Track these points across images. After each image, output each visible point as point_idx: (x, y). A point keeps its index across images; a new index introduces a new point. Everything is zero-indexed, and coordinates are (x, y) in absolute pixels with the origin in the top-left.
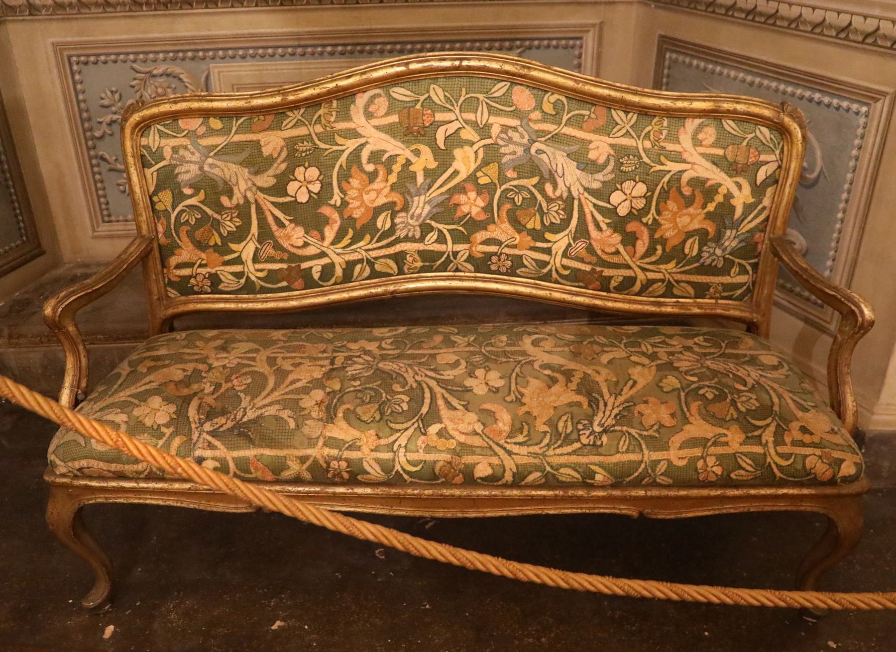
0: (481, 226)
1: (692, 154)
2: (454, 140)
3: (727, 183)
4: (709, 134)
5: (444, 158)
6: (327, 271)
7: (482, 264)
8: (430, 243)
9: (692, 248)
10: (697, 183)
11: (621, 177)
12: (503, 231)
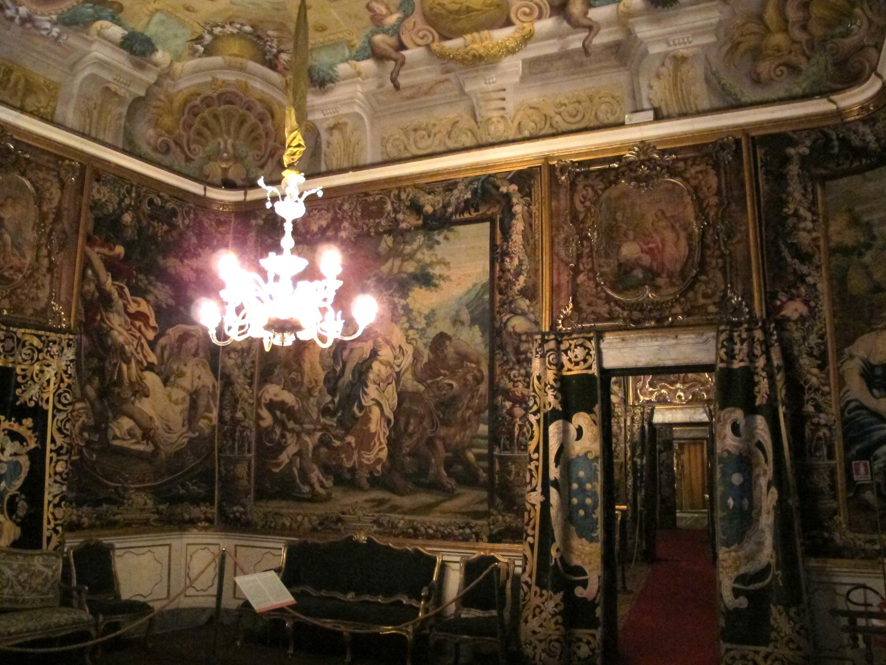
1: (38, 565)
3: (46, 570)
4: (41, 559)
9: (39, 588)
10: (39, 571)
11: (21, 572)
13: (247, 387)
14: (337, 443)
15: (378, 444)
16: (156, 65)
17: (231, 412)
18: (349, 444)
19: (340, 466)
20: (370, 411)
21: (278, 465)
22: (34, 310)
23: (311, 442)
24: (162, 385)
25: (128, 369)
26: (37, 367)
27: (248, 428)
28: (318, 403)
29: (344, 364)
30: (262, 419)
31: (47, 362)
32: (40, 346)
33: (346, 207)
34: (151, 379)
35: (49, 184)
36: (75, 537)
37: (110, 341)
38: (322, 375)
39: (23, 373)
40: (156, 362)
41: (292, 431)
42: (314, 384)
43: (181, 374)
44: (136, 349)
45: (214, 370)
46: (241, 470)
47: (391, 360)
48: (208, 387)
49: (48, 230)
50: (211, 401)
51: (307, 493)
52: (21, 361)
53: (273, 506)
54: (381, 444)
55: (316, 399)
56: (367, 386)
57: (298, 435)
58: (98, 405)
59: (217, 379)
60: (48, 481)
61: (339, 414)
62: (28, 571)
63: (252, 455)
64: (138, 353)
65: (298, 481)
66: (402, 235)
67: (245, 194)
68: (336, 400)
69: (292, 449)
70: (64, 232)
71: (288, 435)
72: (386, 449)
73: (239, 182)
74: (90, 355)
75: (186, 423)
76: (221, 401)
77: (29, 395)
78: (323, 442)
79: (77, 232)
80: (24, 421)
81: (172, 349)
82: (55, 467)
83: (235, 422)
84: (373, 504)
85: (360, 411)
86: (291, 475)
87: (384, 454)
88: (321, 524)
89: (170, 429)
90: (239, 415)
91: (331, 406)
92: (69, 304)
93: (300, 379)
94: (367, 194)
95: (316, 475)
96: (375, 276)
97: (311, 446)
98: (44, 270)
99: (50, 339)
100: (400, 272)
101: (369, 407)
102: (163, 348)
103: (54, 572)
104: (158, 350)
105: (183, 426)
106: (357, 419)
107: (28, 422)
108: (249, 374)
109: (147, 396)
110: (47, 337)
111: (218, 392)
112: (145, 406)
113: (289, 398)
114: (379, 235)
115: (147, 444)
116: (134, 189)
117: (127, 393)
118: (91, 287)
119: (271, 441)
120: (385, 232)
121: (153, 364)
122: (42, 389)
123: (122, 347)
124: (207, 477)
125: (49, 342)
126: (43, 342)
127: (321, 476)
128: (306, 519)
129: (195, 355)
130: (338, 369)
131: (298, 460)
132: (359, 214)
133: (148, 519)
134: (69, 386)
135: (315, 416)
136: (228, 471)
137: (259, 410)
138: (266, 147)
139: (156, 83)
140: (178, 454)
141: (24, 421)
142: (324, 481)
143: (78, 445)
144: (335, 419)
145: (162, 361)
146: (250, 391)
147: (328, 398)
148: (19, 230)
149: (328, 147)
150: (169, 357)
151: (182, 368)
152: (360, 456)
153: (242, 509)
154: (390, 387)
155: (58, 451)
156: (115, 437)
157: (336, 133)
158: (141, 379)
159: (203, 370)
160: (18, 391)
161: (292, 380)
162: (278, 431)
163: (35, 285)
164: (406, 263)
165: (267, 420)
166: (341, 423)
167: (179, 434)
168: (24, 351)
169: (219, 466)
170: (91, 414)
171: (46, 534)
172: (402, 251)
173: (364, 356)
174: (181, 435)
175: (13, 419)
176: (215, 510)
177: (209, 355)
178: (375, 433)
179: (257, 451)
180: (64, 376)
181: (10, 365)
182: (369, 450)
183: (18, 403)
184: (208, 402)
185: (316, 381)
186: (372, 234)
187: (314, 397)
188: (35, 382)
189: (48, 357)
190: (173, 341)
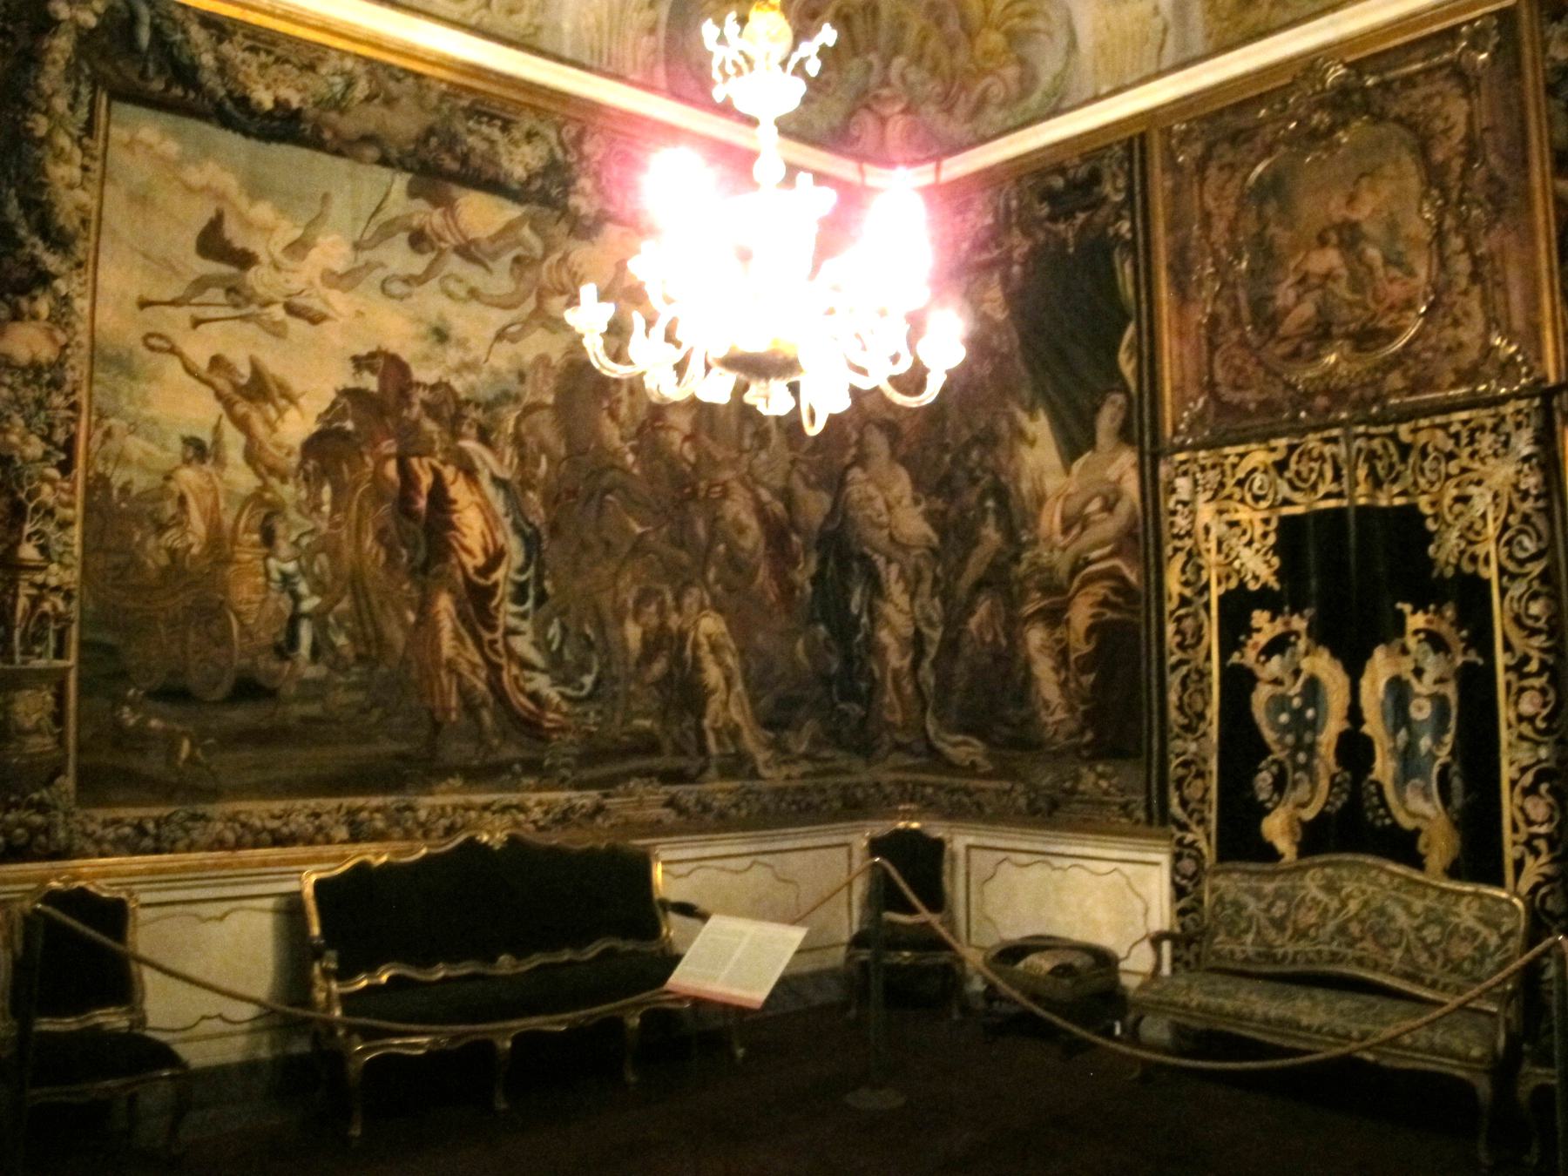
0: (1362, 939)
2: (1349, 896)
3: (1484, 931)
5: (1344, 904)
7: (1360, 962)
8: (1334, 946)
9: (1467, 966)
10: (1468, 929)
11: (1428, 922)
12: (1368, 944)
22: (1456, 371)
31: (1474, 476)
35: (1437, 101)
60: (1505, 735)
62: (1440, 921)
70: (1491, 179)
82: (1516, 703)
92: (1535, 330)
98: (1463, 282)
103: (1505, 938)
148: (1393, 227)
163: (1448, 320)
171: (1510, 853)
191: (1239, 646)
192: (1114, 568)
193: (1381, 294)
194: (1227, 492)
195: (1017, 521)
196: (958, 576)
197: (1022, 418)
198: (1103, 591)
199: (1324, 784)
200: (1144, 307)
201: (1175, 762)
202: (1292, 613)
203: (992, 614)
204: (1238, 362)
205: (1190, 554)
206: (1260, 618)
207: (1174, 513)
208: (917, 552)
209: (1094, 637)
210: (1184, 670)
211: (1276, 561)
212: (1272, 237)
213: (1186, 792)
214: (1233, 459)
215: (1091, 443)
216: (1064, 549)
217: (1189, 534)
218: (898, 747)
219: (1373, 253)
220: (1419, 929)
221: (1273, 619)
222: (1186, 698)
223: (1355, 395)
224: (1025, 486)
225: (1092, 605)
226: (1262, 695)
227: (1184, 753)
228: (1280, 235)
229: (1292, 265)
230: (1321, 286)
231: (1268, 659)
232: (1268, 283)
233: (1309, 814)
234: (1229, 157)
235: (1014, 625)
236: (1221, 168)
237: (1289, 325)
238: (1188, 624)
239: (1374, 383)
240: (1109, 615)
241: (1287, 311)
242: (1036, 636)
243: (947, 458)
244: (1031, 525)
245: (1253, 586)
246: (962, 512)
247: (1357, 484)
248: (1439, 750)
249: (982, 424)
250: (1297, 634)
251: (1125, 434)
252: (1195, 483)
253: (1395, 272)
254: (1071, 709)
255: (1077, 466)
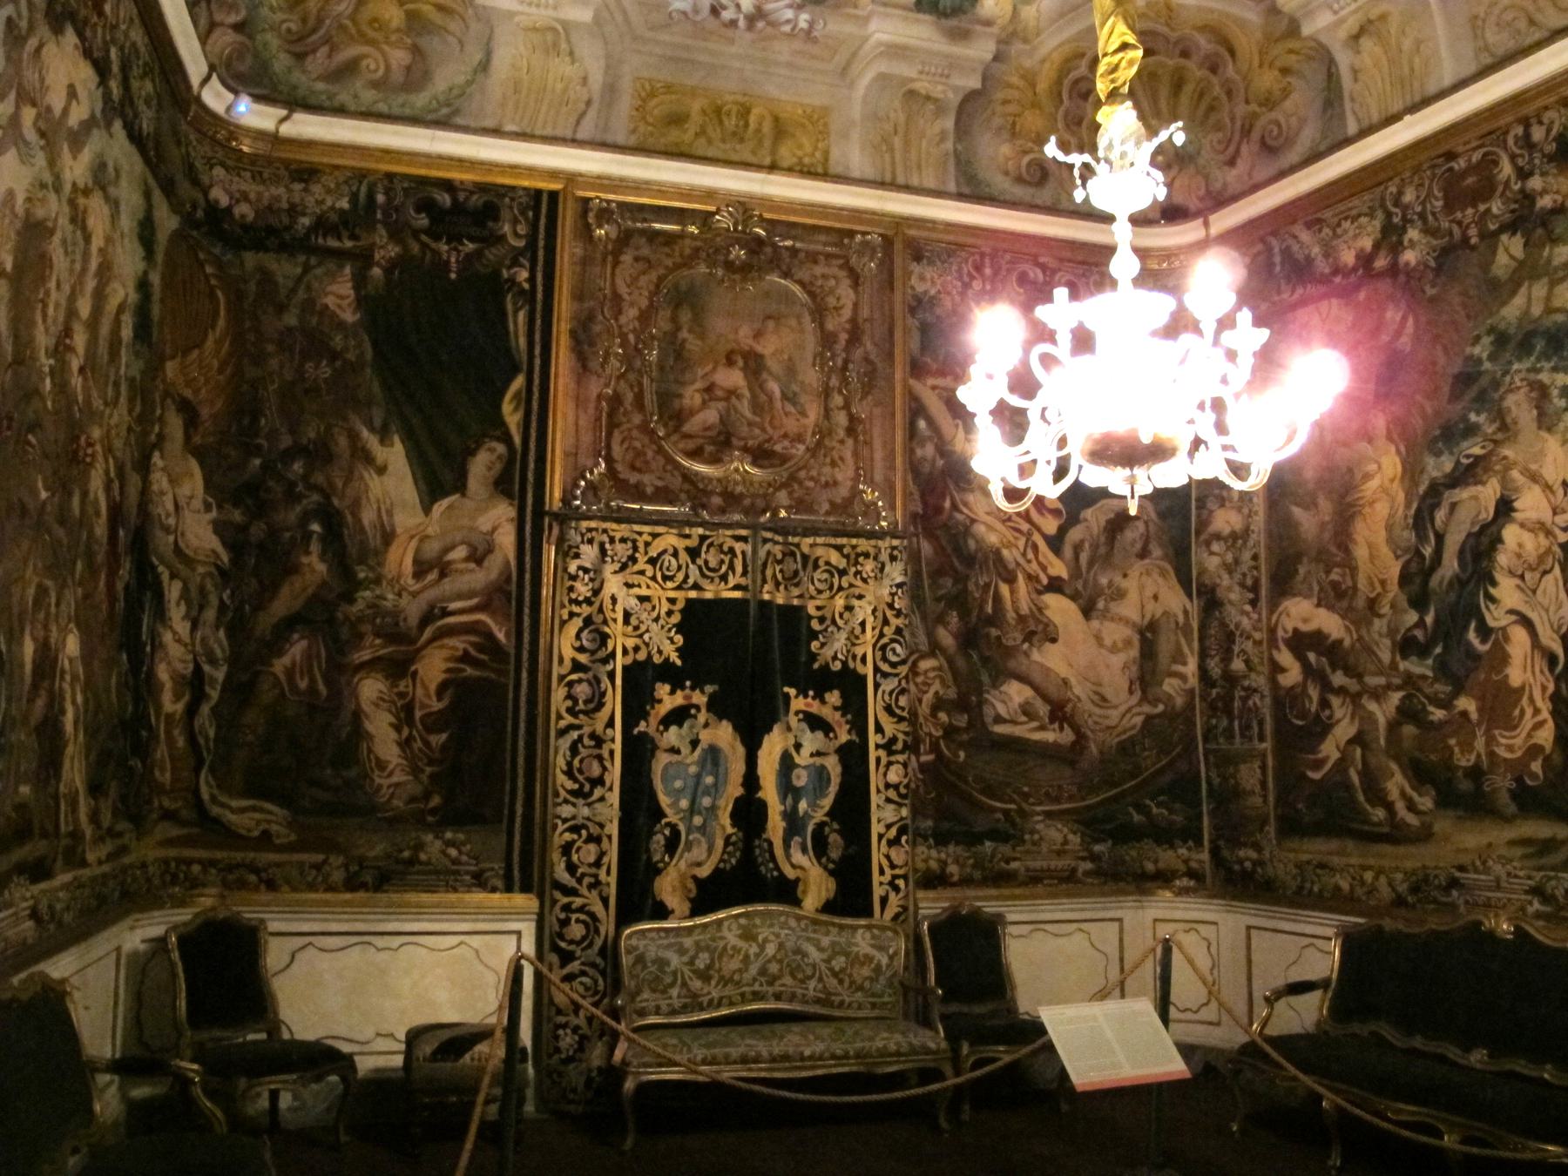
1: (862, 944)
2: (766, 941)
4: (868, 935)
5: (762, 947)
6: (711, 1002)
7: (778, 997)
8: (757, 987)
12: (788, 980)
13: (1248, 608)
14: (1438, 714)
15: (1529, 712)
16: (988, 23)
17: (1223, 660)
18: (1464, 714)
19: (1449, 766)
20: (1507, 639)
21: (1318, 764)
22: (832, 503)
23: (1382, 712)
24: (1080, 616)
25: (1012, 592)
26: (840, 602)
27: (1255, 691)
28: (1391, 632)
29: (1440, 538)
30: (1283, 670)
31: (857, 591)
32: (842, 564)
33: (1409, 196)
34: (1059, 608)
35: (832, 282)
36: (935, 900)
37: (972, 544)
38: (1394, 570)
39: (819, 613)
40: (1065, 575)
41: (1341, 691)
42: (1379, 589)
43: (1120, 595)
44: (1024, 554)
45: (1185, 581)
46: (1248, 776)
47: (1547, 516)
48: (1175, 616)
49: (840, 362)
50: (1183, 641)
51: (1379, 824)
52: (814, 593)
53: (1314, 849)
54: (1537, 711)
55: (1385, 621)
56: (1494, 583)
57: (1355, 698)
58: (961, 663)
59: (1190, 596)
60: (875, 799)
61: (1438, 650)
63: (1267, 745)
64: (1029, 561)
65: (1361, 798)
66: (1544, 224)
67: (1206, 224)
68: (1429, 619)
69: (1344, 730)
70: (867, 360)
71: (1335, 701)
72: (1550, 724)
73: (1193, 204)
74: (937, 574)
75: (1137, 686)
76: (1201, 639)
77: (831, 649)
78: (1409, 713)
79: (890, 355)
80: (827, 696)
81: (1095, 547)
82: (885, 774)
83: (1231, 679)
84: (1530, 850)
85: (1484, 641)
86: (1348, 786)
87: (1546, 736)
88: (1415, 889)
89: (1104, 699)
90: (1238, 665)
91: (1419, 634)
92: (892, 487)
93: (1350, 583)
94: (1451, 156)
95: (1396, 783)
96: (1492, 330)
97: (1382, 721)
98: (841, 433)
99: (859, 550)
100: (1549, 310)
101: (1504, 629)
102: (1077, 548)
104: (1068, 551)
105: (1131, 692)
106: (1475, 657)
107: (834, 697)
108: (1249, 582)
109: (1054, 640)
110: (854, 547)
111: (1195, 625)
112: (1051, 659)
113: (1331, 624)
114: (1490, 238)
115: (1062, 729)
116: (987, 260)
117: (1014, 637)
118: (929, 451)
119: (1303, 714)
120: (1503, 229)
121: (1059, 578)
122: (853, 639)
123: (998, 553)
124: (1183, 789)
125: (858, 555)
126: (847, 557)
127: (1408, 790)
128: (1383, 880)
129: (1143, 554)
130: (1428, 551)
131: (1358, 752)
132: (1439, 204)
133: (1074, 870)
134: (898, 631)
135: (1385, 656)
136: (1225, 779)
137: (1275, 653)
138: (1233, 119)
139: (997, 58)
140: (1126, 748)
141: (827, 696)
142: (1415, 795)
143: (930, 735)
144: (1430, 662)
145: (1076, 572)
146: (1255, 616)
147: (1412, 617)
148: (791, 370)
149: (1356, 80)
150: (1091, 563)
151: (1118, 579)
152: (1491, 740)
153: (1253, 855)
154: (1549, 577)
155: (888, 747)
156: (999, 720)
157: (1367, 43)
158: (1040, 610)
159: (1160, 580)
160: (814, 645)
161: (1335, 585)
162: (1314, 693)
163: (828, 460)
164: (1559, 289)
165: (1293, 674)
166: (1443, 669)
167: (1123, 708)
168: (817, 575)
169: (1208, 770)
170: (949, 677)
171: (878, 892)
172: (1549, 261)
173: (1483, 516)
174: (1129, 710)
175: (811, 693)
176: (1205, 856)
177: (1171, 551)
178: (1522, 688)
179: (1278, 732)
180: (889, 613)
181: (796, 602)
182: (1511, 725)
183: (816, 666)
184: (1178, 643)
185: (1383, 583)
186: (1474, 241)
187: (1380, 616)
188: (839, 628)
189: (859, 583)
190: (1095, 531)
191: (645, 716)
192: (477, 622)
193: (776, 423)
194: (636, 568)
195: (353, 550)
196: (259, 607)
197: (371, 440)
198: (461, 646)
199: (720, 843)
200: (537, 362)
201: (561, 828)
202: (693, 688)
203: (309, 656)
204: (638, 444)
205: (588, 621)
206: (663, 690)
207: (574, 578)
208: (201, 570)
209: (449, 693)
210: (575, 735)
211: (679, 639)
212: (684, 341)
213: (575, 858)
214: (646, 537)
215: (460, 486)
216: (414, 595)
217: (588, 601)
218: (169, 816)
219: (774, 387)
220: (828, 961)
221: (673, 692)
222: (576, 763)
223: (747, 502)
224: (368, 517)
225: (448, 660)
226: (661, 760)
227: (574, 818)
228: (693, 344)
229: (700, 372)
230: (727, 399)
231: (666, 729)
232: (677, 381)
233: (704, 872)
234: (645, 251)
235: (339, 671)
236: (637, 259)
237: (693, 425)
238: (582, 690)
239: (765, 496)
240: (469, 671)
241: (692, 413)
242: (371, 688)
243: (257, 462)
244: (372, 562)
245: (657, 659)
246: (273, 532)
247: (764, 581)
248: (817, 810)
249: (312, 435)
250: (698, 708)
251: (503, 485)
252: (603, 552)
253: (790, 408)
254: (415, 771)
255: (440, 507)
